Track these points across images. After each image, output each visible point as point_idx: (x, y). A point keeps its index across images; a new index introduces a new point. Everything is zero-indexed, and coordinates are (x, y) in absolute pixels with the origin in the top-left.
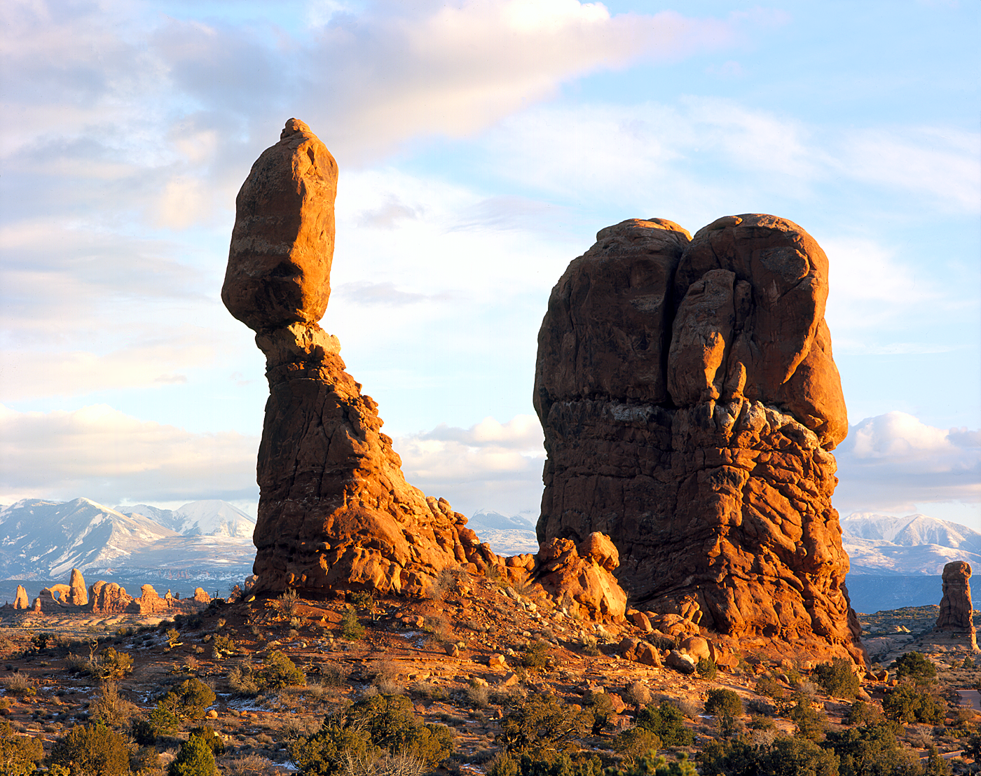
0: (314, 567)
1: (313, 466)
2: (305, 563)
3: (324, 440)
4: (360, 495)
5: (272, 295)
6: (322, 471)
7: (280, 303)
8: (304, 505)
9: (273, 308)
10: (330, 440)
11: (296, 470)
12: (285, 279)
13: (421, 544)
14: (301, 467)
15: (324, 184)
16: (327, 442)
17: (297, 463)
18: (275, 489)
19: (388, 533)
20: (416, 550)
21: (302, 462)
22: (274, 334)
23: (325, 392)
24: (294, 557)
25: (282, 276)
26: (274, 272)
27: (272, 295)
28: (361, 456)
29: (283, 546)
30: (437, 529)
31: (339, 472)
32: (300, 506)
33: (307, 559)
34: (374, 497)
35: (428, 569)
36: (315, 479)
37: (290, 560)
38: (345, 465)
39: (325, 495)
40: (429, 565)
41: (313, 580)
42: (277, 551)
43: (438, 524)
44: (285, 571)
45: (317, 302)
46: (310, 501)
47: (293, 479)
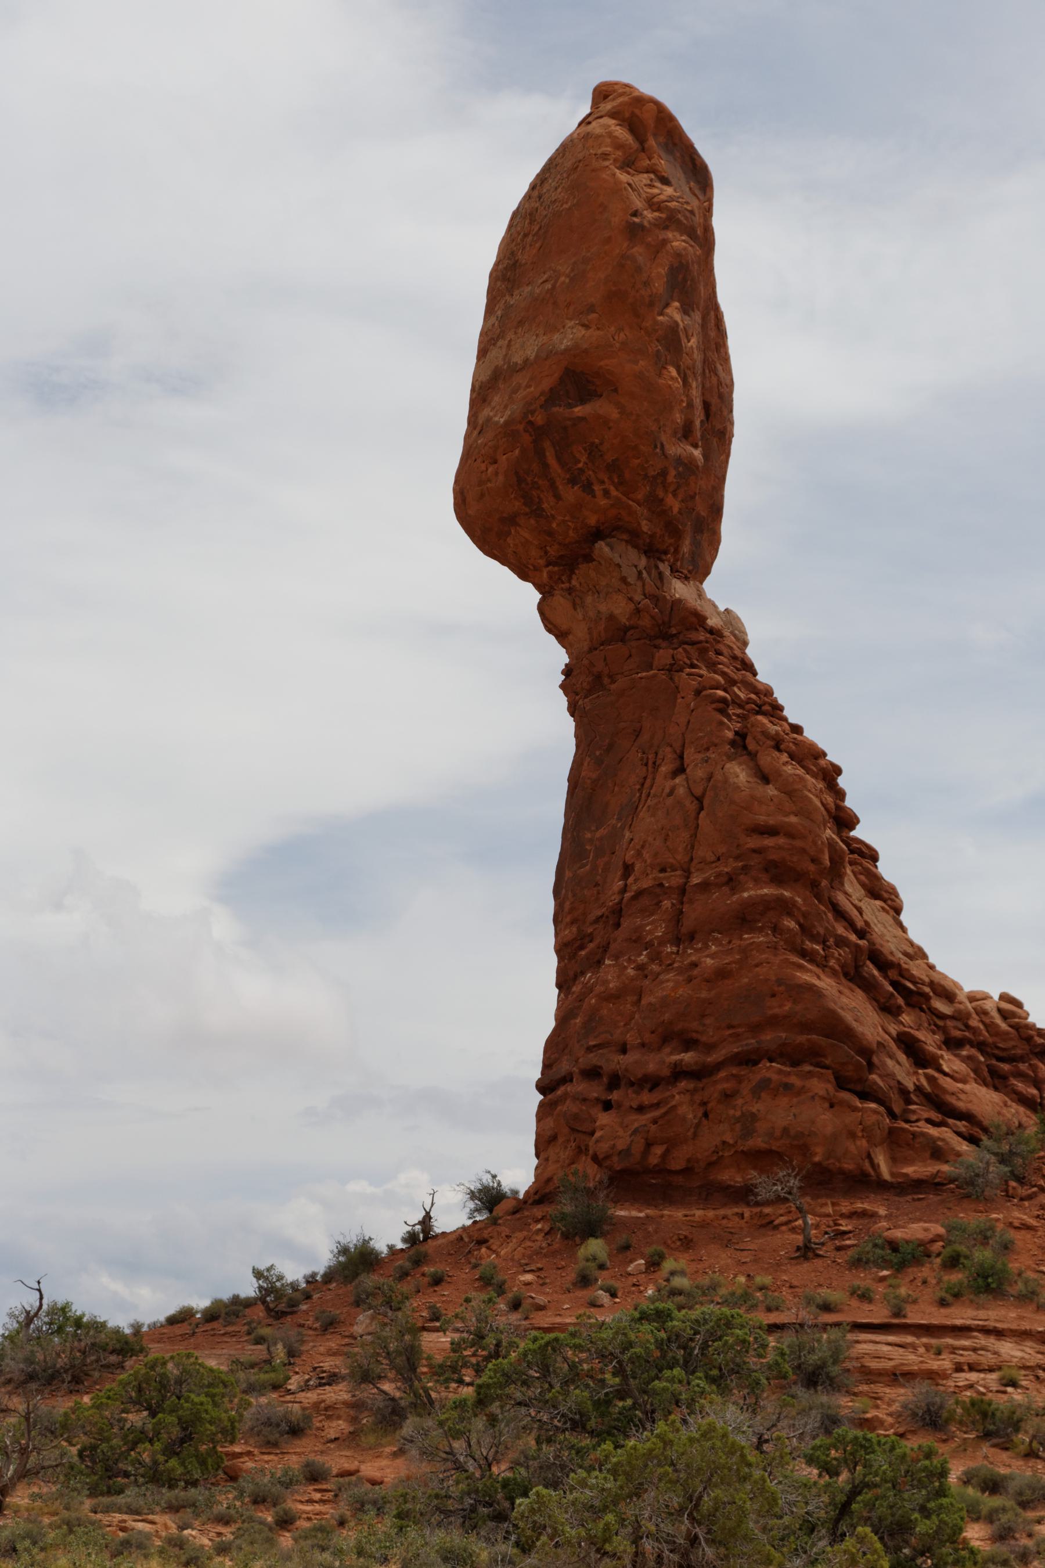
0: (666, 1113)
1: (663, 870)
2: (641, 1109)
3: (687, 803)
4: (776, 929)
5: (551, 460)
6: (682, 881)
7: (573, 481)
8: (640, 968)
9: (558, 497)
10: (700, 800)
11: (624, 890)
12: (578, 411)
13: (946, 1068)
14: (636, 880)
15: (669, 191)
16: (691, 806)
17: (628, 870)
18: (582, 947)
19: (848, 1017)
20: (931, 1079)
21: (638, 866)
22: (574, 582)
23: (691, 696)
24: (615, 1096)
25: (571, 406)
26: (552, 397)
27: (551, 460)
28: (772, 831)
29: (592, 1073)
30: (994, 1062)
31: (724, 879)
32: (631, 972)
33: (646, 1098)
34: (814, 938)
35: (962, 1125)
36: (666, 904)
37: (607, 1106)
38: (737, 858)
39: (692, 937)
40: (967, 1117)
41: (658, 1150)
42: (578, 1087)
43: (996, 1052)
44: (592, 1134)
45: (664, 473)
46: (656, 957)
47: (618, 912)
